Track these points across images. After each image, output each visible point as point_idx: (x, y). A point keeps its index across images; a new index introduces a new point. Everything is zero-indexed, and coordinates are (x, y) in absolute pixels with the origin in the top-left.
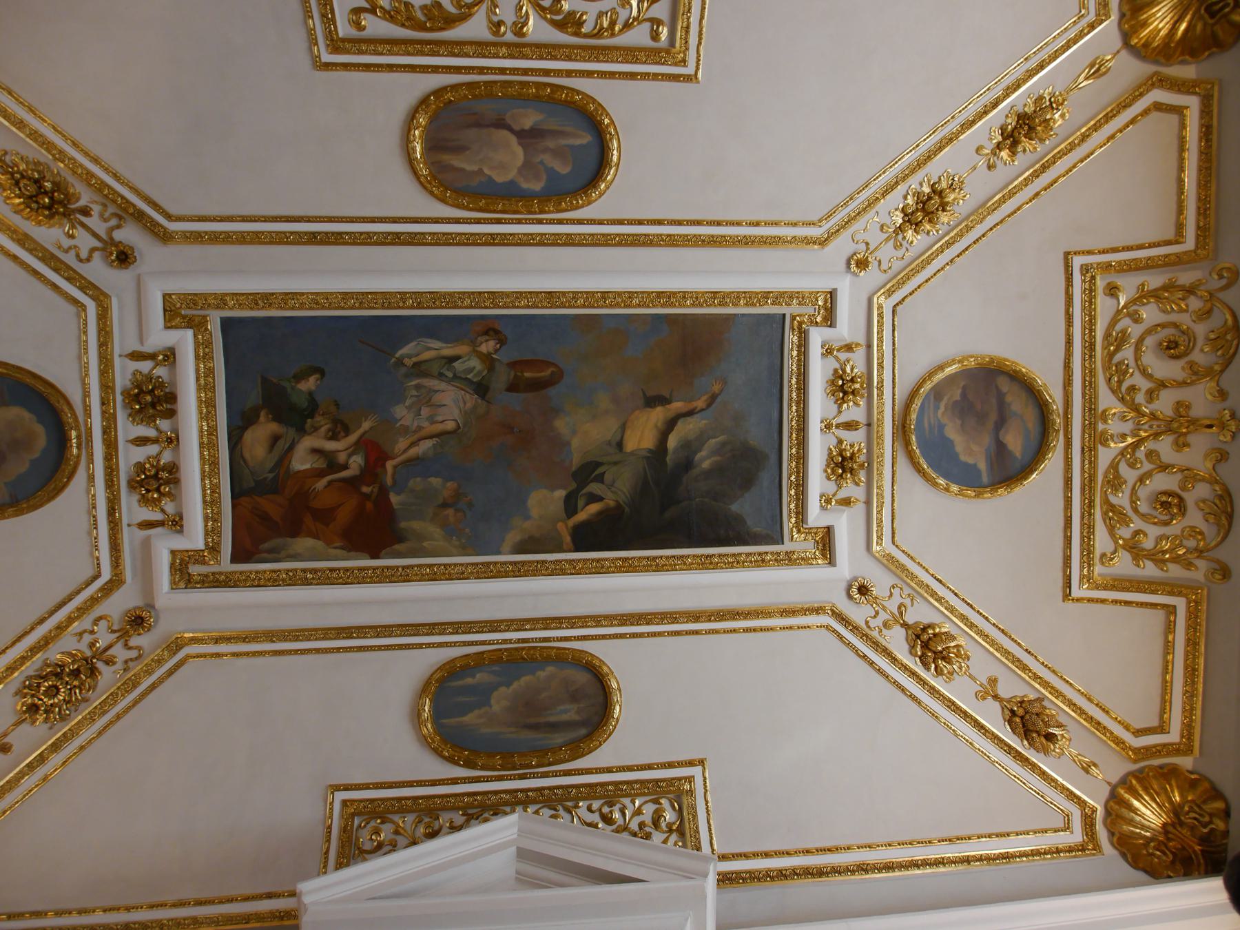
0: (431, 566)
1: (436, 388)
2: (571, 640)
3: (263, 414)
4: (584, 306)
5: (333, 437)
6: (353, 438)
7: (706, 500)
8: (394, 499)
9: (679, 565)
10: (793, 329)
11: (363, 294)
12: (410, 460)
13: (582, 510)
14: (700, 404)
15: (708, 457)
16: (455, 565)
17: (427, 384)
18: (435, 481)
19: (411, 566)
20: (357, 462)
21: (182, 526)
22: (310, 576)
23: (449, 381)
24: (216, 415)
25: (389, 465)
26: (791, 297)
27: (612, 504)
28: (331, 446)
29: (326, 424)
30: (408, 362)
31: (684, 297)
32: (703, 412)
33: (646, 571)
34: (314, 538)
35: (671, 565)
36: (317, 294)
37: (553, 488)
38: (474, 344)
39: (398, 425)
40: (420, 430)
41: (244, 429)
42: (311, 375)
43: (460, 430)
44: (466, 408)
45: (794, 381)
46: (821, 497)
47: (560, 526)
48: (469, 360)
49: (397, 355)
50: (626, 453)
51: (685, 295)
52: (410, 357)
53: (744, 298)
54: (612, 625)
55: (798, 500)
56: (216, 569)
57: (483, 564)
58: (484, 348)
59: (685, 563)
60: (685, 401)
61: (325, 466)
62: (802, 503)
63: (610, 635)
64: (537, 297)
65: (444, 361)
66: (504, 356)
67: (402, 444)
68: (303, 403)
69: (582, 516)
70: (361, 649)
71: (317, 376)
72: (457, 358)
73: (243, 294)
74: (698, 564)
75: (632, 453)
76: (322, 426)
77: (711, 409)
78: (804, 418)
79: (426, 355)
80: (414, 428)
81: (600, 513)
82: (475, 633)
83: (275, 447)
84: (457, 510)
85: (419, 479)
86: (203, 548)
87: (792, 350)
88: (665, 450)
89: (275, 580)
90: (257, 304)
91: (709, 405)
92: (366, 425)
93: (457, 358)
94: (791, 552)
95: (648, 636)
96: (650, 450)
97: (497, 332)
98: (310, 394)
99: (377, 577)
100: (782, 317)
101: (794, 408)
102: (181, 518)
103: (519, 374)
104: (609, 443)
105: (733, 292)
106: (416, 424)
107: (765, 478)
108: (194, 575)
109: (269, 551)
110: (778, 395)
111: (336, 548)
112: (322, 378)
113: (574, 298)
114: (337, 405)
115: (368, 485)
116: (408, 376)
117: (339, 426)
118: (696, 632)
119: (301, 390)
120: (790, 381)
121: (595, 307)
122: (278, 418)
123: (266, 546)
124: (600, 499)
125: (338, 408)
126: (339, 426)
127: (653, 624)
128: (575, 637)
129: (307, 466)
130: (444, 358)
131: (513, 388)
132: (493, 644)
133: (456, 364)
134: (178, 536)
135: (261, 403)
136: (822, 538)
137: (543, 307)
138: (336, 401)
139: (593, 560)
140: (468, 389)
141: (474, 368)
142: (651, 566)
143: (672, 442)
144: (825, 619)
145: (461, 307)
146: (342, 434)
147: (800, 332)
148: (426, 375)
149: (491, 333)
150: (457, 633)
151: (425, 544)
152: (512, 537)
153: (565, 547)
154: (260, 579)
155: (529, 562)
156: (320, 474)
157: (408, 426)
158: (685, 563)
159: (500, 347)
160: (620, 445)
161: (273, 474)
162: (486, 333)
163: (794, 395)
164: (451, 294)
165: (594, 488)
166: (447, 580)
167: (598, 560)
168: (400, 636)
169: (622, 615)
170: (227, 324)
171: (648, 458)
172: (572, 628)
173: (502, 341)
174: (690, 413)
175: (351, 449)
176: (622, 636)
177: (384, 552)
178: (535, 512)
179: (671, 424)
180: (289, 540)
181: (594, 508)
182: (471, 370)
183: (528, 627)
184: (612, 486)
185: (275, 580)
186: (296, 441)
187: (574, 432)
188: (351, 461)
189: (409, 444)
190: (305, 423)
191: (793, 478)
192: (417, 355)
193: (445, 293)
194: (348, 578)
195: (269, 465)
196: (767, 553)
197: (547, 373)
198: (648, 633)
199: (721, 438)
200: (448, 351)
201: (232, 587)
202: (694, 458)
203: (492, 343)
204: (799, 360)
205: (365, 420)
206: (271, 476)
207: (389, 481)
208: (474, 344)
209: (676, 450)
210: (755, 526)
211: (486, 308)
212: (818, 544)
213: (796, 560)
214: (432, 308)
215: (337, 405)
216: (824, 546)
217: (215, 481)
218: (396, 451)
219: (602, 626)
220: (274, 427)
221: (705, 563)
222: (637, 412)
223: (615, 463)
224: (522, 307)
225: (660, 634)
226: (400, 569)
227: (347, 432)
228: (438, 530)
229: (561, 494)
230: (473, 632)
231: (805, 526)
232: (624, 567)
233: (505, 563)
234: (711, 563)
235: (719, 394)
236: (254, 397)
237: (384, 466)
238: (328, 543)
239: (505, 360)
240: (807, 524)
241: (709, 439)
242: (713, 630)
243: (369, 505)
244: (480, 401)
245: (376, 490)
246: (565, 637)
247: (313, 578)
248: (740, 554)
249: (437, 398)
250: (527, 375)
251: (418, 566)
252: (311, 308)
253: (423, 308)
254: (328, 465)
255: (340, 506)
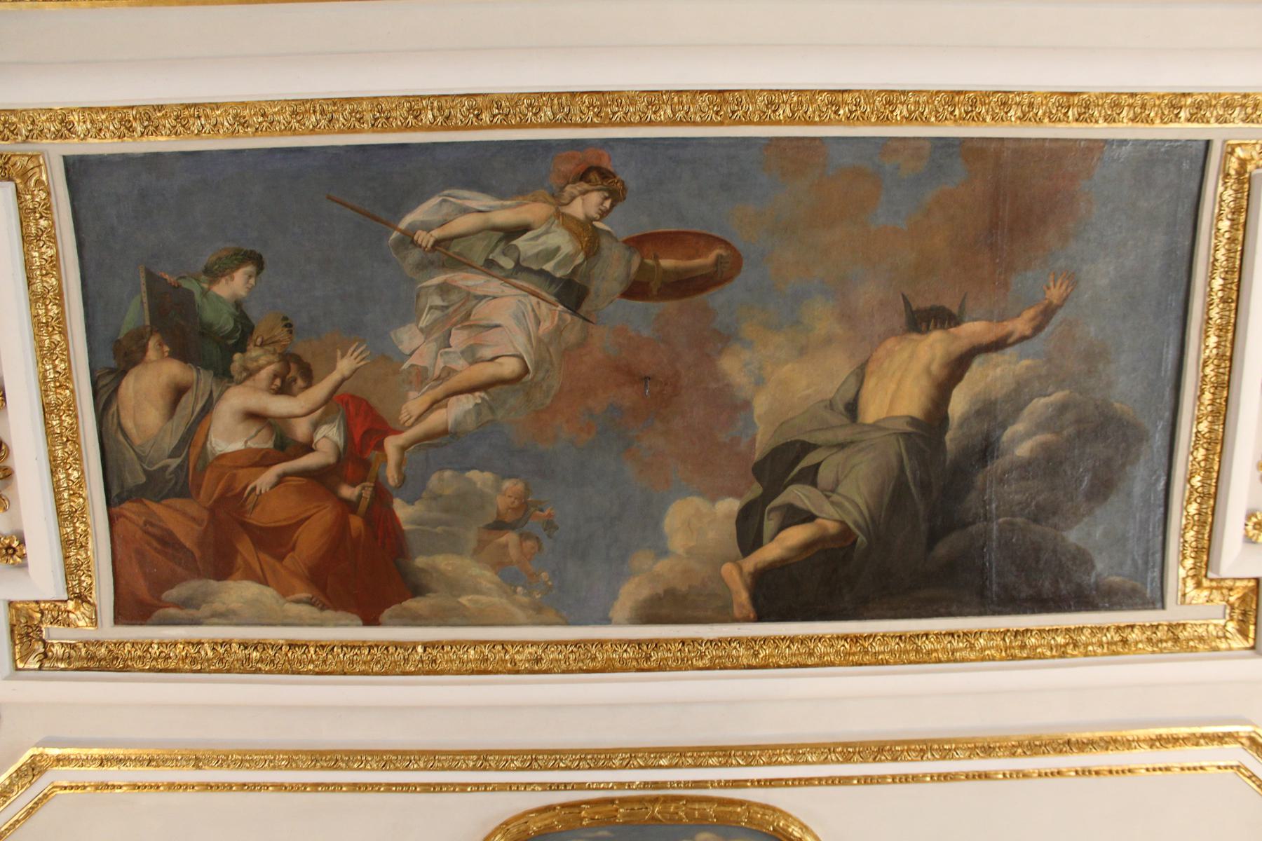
0: (476, 644)
1: (479, 292)
2: (746, 787)
3: (152, 343)
4: (791, 121)
5: (284, 389)
6: (320, 391)
7: (1019, 520)
8: (402, 511)
9: (961, 650)
10: (1227, 175)
11: (334, 102)
12: (430, 436)
13: (772, 538)
14: (1020, 325)
15: (1028, 435)
16: (524, 644)
17: (460, 283)
18: (480, 478)
19: (438, 642)
20: (329, 438)
21: (23, 557)
22: (255, 655)
23: (507, 277)
24: (67, 349)
25: (392, 444)
26: (1228, 105)
27: (832, 527)
28: (280, 406)
29: (269, 363)
30: (424, 238)
31: (1004, 104)
32: (1025, 344)
33: (895, 663)
34: (260, 583)
35: (944, 650)
36: (244, 104)
37: (714, 496)
38: (557, 198)
39: (406, 366)
40: (449, 374)
41: (120, 373)
42: (238, 268)
43: (529, 377)
44: (541, 332)
45: (1217, 283)
46: (1248, 517)
47: (728, 570)
48: (547, 232)
49: (403, 225)
50: (864, 425)
51: (1004, 100)
52: (428, 228)
53: (1130, 106)
54: (825, 761)
55: (1202, 524)
56: (91, 633)
57: (577, 644)
58: (578, 209)
59: (972, 647)
60: (990, 320)
61: (270, 445)
62: (1211, 530)
63: (820, 779)
64: (693, 102)
65: (501, 234)
66: (622, 224)
67: (415, 403)
68: (226, 322)
69: (771, 552)
70: (356, 787)
71: (249, 268)
72: (522, 229)
73: (103, 110)
74: (997, 648)
75: (876, 426)
76: (260, 368)
77: (1043, 335)
78: (1231, 359)
79: (462, 224)
80: (437, 373)
81: (807, 546)
82: (563, 769)
83: (178, 409)
84: (524, 537)
85: (447, 474)
86: (65, 597)
87: (1219, 217)
88: (945, 419)
89: (194, 661)
90: (131, 129)
91: (1038, 329)
92: (345, 366)
93: (522, 229)
94: (1179, 625)
95: (894, 781)
96: (912, 418)
97: (605, 175)
98: (238, 304)
99: (378, 662)
100: (1202, 147)
101: (1213, 340)
102: (22, 542)
103: (649, 262)
104: (831, 405)
105: (1107, 95)
106: (440, 364)
107: (1139, 478)
108: (52, 645)
109: (183, 604)
110: (1180, 313)
111: (298, 602)
112: (258, 273)
113: (770, 103)
114: (289, 326)
115: (354, 486)
116: (425, 266)
117: (293, 367)
118: (985, 776)
119: (218, 297)
120: (1210, 284)
121: (815, 123)
122: (181, 353)
123: (173, 594)
124: (809, 517)
125: (291, 332)
126: (293, 367)
127: (905, 760)
128: (752, 781)
129: (238, 446)
130: (495, 229)
131: (636, 290)
132: (597, 789)
133: (521, 243)
134: (18, 573)
135: (148, 323)
136: (1243, 599)
137: (704, 123)
138: (285, 318)
139: (792, 640)
140: (544, 294)
141: (558, 249)
142: (907, 652)
143: (958, 404)
144: (1235, 754)
145: (533, 126)
146: (300, 383)
147: (1240, 181)
148: (458, 263)
149: (594, 176)
150: (530, 768)
151: (464, 600)
152: (632, 592)
153: (737, 612)
154: (167, 658)
155: (667, 641)
156: (263, 461)
157: (426, 369)
158: (972, 647)
159: (612, 206)
160: (852, 409)
161: (178, 461)
162: (583, 177)
163: (1214, 313)
164: (515, 99)
165: (797, 495)
166: (510, 672)
167: (803, 641)
168: (425, 769)
169: (846, 745)
170: (76, 169)
171: (907, 435)
172: (749, 765)
173: (616, 195)
174: (998, 345)
175: (319, 412)
176: (845, 781)
177: (387, 612)
178: (678, 542)
179: (958, 367)
180: (214, 584)
181: (796, 535)
182: (551, 254)
183: (663, 762)
184: (833, 491)
185: (194, 661)
186: (215, 395)
187: (760, 382)
188: (318, 436)
189: (425, 406)
190: (231, 361)
191: (1196, 481)
192: (442, 225)
193: (500, 96)
194: (324, 662)
195: (170, 442)
196: (1132, 627)
197: (706, 260)
198: (894, 777)
199: (1058, 396)
200: (506, 216)
201: (121, 670)
202: (999, 439)
203: (595, 198)
204: (1232, 240)
205: (343, 356)
206: (175, 463)
207: (391, 475)
208: (557, 198)
209: (965, 420)
210: (1105, 569)
211: (584, 125)
212: (1232, 608)
213: (1188, 640)
214: (473, 128)
215: (289, 326)
216: (1244, 613)
217: (76, 474)
218: (404, 417)
219: (807, 762)
220: (174, 370)
221: (1012, 647)
222: (890, 343)
223: (841, 446)
224: (661, 124)
225: (916, 778)
226: (420, 649)
227: (309, 378)
228: (489, 574)
229: (730, 506)
230: (559, 768)
231: (1210, 575)
232: (854, 654)
233: (621, 642)
234: (1023, 647)
235: (1060, 306)
236: (135, 313)
237: (380, 447)
238: (285, 593)
239: (623, 234)
240: (1217, 573)
241: (1031, 399)
242: (1018, 772)
243: (356, 523)
244: (568, 317)
245: (367, 494)
246: (735, 781)
247: (261, 660)
248: (1080, 630)
249: (482, 312)
250: (666, 263)
251: (453, 644)
252: (234, 134)
253: (456, 128)
254: (275, 445)
255: (300, 523)
